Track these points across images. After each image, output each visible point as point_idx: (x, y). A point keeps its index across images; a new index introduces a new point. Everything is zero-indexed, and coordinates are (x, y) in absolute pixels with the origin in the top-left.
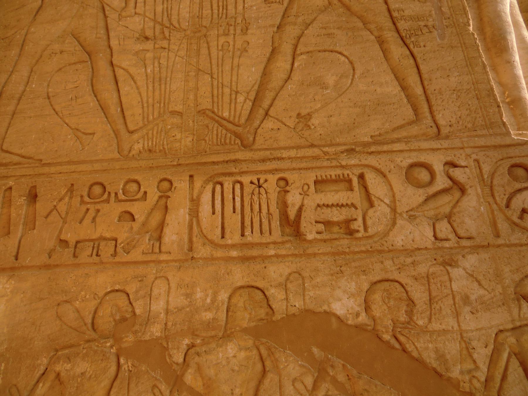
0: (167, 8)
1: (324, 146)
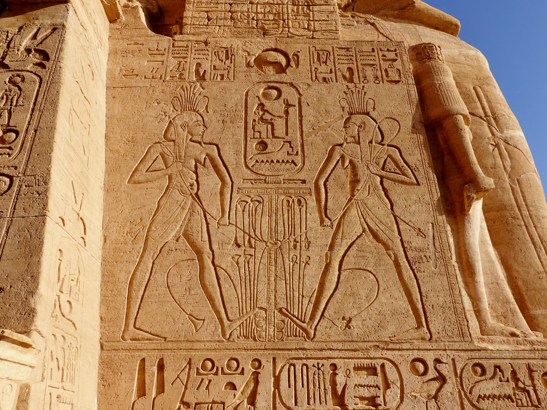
0: (252, 221)
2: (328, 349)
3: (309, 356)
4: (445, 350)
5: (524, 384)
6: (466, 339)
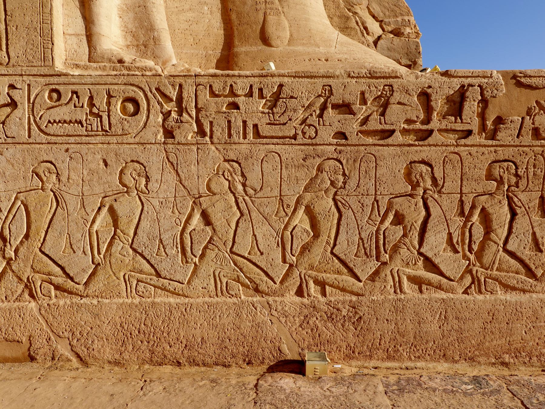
4: (22, 75)
5: (98, 110)
6: (47, 63)
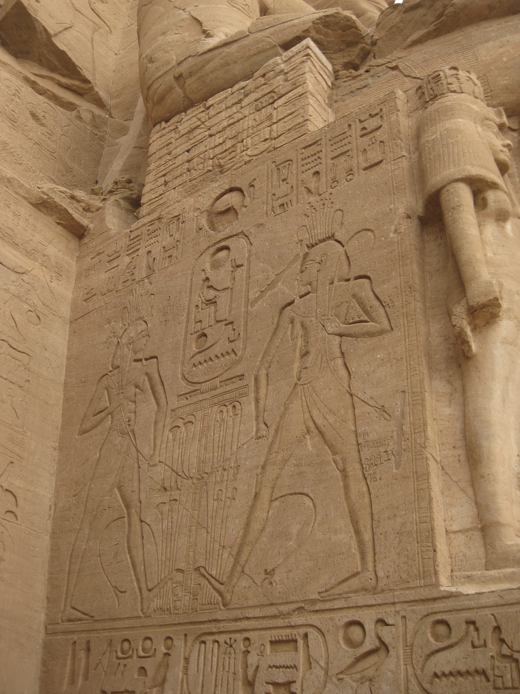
1: (281, 604)
2: (244, 618)
3: (222, 629)
